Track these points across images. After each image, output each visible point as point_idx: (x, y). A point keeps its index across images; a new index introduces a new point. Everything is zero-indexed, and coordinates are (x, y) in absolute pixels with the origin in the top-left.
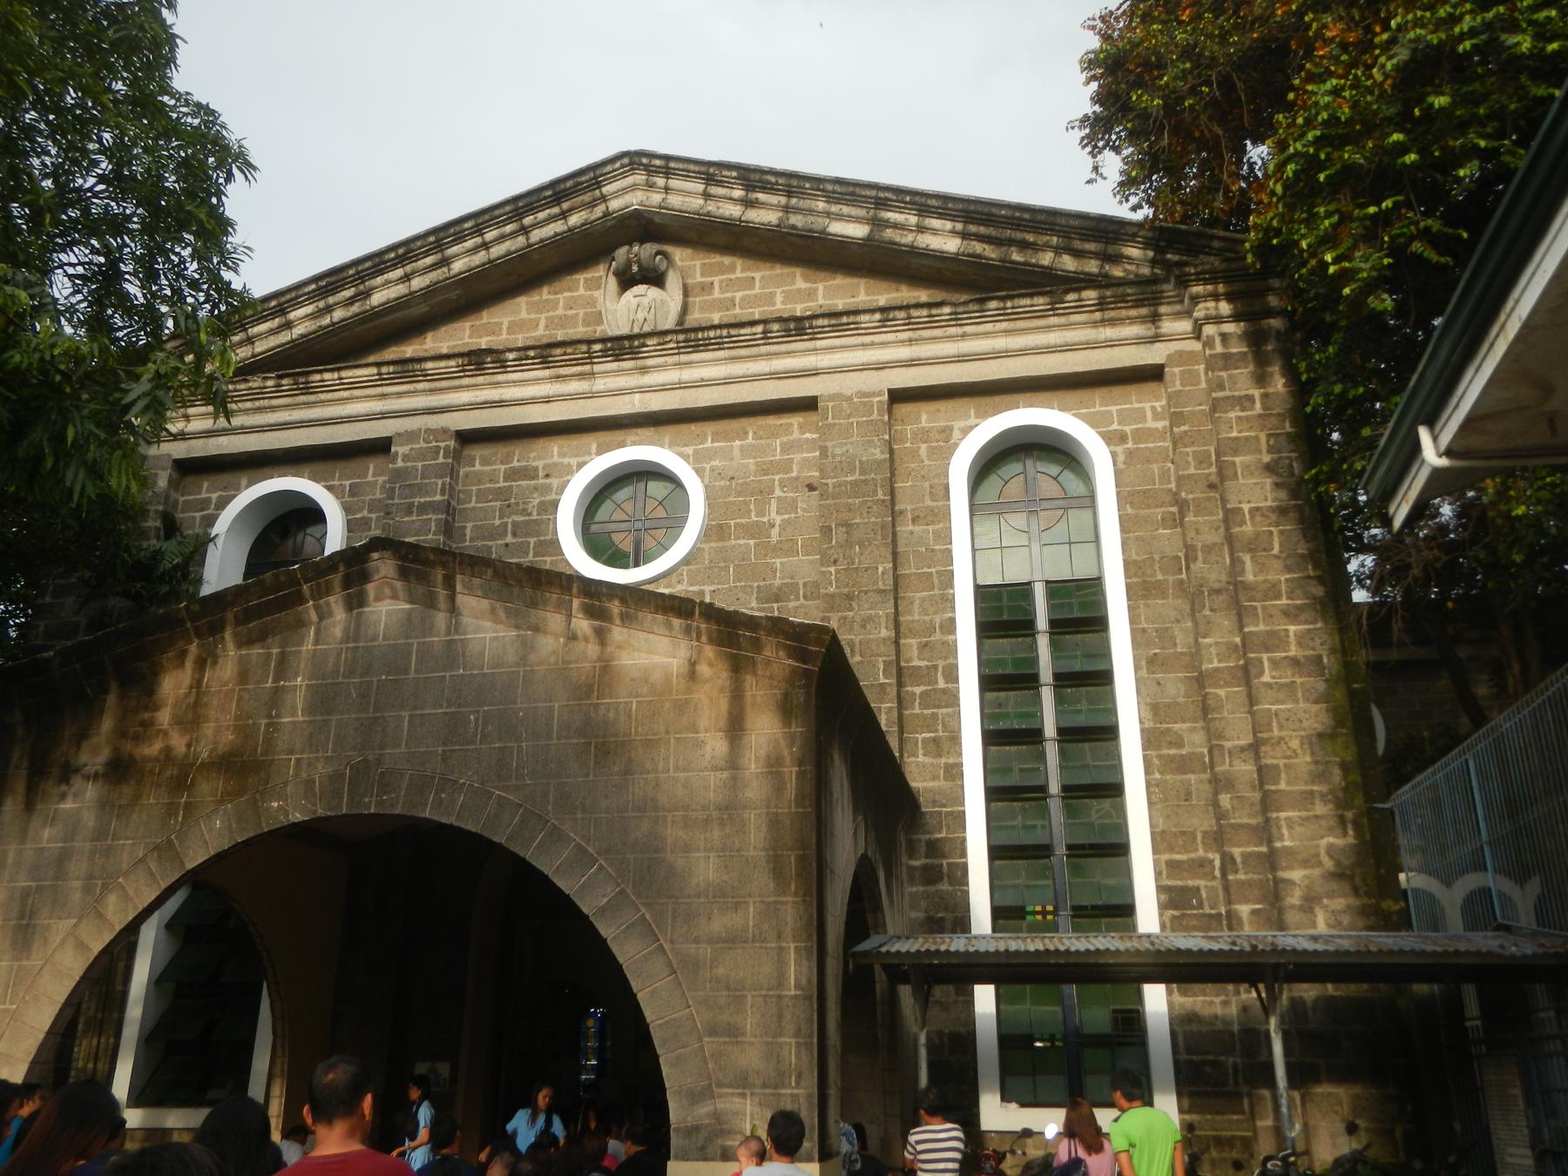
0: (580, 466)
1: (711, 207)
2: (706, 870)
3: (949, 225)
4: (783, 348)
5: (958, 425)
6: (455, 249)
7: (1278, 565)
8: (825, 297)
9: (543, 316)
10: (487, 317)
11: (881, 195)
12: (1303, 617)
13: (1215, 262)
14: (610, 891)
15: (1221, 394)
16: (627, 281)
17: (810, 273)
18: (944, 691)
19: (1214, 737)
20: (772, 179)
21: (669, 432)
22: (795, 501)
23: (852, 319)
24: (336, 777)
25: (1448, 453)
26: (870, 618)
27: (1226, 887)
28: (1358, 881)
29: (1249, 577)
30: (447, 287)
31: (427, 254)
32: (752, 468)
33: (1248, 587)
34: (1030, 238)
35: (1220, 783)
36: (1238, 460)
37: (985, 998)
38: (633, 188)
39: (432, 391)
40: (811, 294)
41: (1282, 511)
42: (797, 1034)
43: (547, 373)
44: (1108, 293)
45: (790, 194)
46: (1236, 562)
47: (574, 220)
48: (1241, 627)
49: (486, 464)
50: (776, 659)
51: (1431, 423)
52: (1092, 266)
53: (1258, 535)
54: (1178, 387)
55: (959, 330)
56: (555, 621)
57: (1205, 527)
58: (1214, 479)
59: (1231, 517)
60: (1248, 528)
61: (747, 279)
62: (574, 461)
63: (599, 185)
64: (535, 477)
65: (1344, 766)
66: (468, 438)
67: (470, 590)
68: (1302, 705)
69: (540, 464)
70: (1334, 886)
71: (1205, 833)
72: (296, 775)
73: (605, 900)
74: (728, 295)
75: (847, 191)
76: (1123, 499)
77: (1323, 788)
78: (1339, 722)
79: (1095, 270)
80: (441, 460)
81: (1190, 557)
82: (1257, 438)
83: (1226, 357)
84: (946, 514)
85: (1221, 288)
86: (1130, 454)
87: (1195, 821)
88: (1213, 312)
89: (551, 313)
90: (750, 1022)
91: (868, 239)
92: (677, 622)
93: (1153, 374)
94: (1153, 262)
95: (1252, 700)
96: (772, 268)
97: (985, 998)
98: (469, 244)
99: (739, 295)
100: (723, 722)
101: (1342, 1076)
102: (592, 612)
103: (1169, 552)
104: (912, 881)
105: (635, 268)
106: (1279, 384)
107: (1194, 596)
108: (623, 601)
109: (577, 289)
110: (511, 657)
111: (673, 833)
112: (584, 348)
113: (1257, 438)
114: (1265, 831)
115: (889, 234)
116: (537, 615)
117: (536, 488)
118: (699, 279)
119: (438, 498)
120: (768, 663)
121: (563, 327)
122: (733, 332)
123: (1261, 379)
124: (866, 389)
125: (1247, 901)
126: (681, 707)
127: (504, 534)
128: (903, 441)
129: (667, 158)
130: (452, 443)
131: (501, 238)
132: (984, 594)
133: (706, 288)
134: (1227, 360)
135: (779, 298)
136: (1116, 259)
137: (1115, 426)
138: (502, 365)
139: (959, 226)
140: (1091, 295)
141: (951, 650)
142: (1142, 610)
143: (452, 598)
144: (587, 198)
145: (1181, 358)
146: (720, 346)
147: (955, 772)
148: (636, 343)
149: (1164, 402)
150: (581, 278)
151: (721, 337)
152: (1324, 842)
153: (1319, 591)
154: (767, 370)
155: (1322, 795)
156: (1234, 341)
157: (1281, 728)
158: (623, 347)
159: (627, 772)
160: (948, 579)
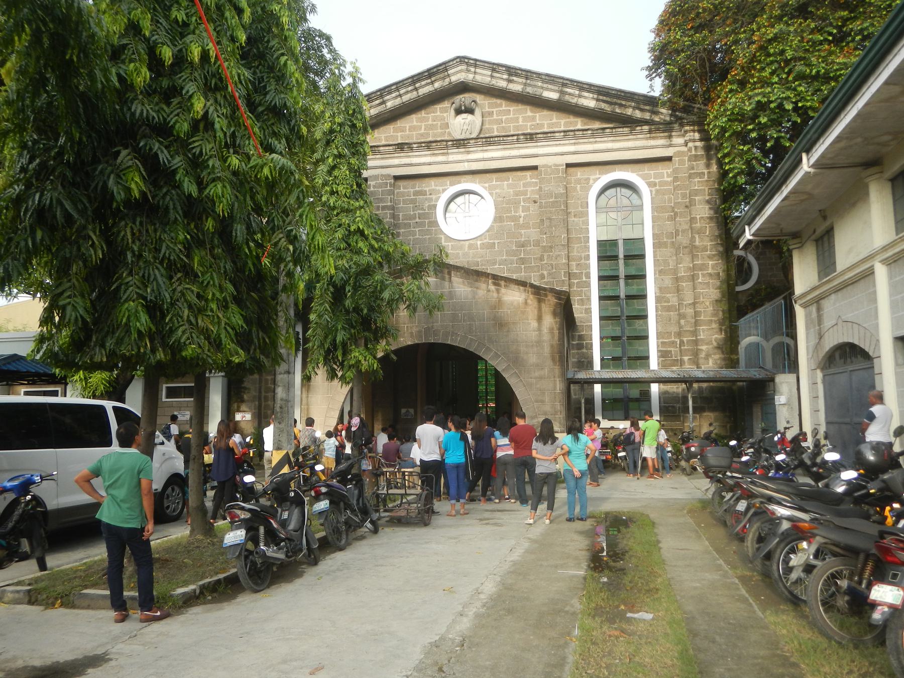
0: (444, 190)
1: (494, 82)
2: (532, 359)
3: (591, 95)
4: (525, 145)
5: (592, 177)
6: (388, 97)
7: (708, 239)
8: (539, 120)
10: (400, 123)
11: (565, 82)
12: (715, 258)
13: (695, 118)
14: (505, 365)
15: (693, 171)
16: (459, 112)
17: (534, 109)
18: (585, 282)
19: (681, 300)
20: (520, 72)
21: (478, 177)
22: (529, 207)
23: (552, 135)
24: (420, 332)
25: (753, 235)
26: (559, 255)
27: (681, 351)
28: (724, 349)
29: (697, 243)
31: (376, 99)
32: (512, 193)
33: (696, 247)
34: (624, 103)
35: (682, 316)
36: (696, 198)
37: (598, 388)
38: (461, 71)
39: (382, 158)
40: (534, 119)
41: (711, 218)
42: (560, 402)
43: (429, 152)
44: (653, 127)
45: (527, 79)
46: (693, 237)
47: (437, 85)
48: (693, 262)
49: (405, 188)
50: (552, 300)
51: (749, 224)
52: (647, 116)
53: (701, 227)
54: (677, 166)
55: (594, 140)
56: (484, 286)
57: (683, 223)
58: (688, 204)
59: (692, 220)
60: (698, 225)
62: (441, 188)
63: (447, 70)
64: (425, 195)
65: (723, 311)
66: (397, 178)
67: (456, 276)
68: (712, 290)
69: (427, 189)
70: (716, 351)
71: (675, 332)
72: (407, 330)
74: (500, 117)
75: (550, 79)
76: (654, 209)
77: (716, 319)
78: (723, 296)
79: (648, 118)
80: (389, 188)
81: (677, 234)
82: (704, 190)
83: (696, 156)
84: (587, 214)
85: (696, 128)
86: (657, 191)
87: (672, 328)
88: (692, 138)
90: (547, 399)
91: (559, 100)
92: (522, 288)
93: (669, 159)
94: (671, 115)
95: (694, 288)
96: (517, 106)
97: (598, 388)
98: (394, 95)
99: (504, 118)
100: (536, 317)
101: (712, 410)
102: (495, 284)
103: (670, 230)
104: (573, 349)
105: (463, 108)
106: (714, 168)
107: (677, 249)
108: (505, 281)
109: (437, 112)
110: (470, 296)
111: (523, 349)
112: (445, 143)
113: (704, 190)
114: (695, 333)
115: (567, 98)
116: (477, 284)
117: (426, 199)
118: (487, 110)
119: (389, 204)
120: (549, 300)
121: (432, 129)
122: (505, 139)
123: (708, 166)
124: (557, 163)
125: (687, 356)
126: (523, 313)
127: (415, 218)
128: (571, 183)
129: (476, 60)
130: (392, 181)
131: (407, 92)
132: (601, 244)
133: (490, 114)
134: (696, 158)
135: (521, 120)
136: (656, 113)
137: (652, 180)
138: (411, 149)
139: (595, 96)
140: (646, 128)
141: (588, 266)
142: (658, 253)
143: (450, 278)
144: (442, 75)
145: (679, 154)
146: (499, 144)
147: (589, 311)
149: (671, 170)
150: (438, 107)
152: (714, 337)
153: (721, 249)
154: (518, 154)
155: (715, 321)
156: (699, 149)
157: (703, 298)
158: (460, 143)
159: (508, 331)
160: (587, 239)
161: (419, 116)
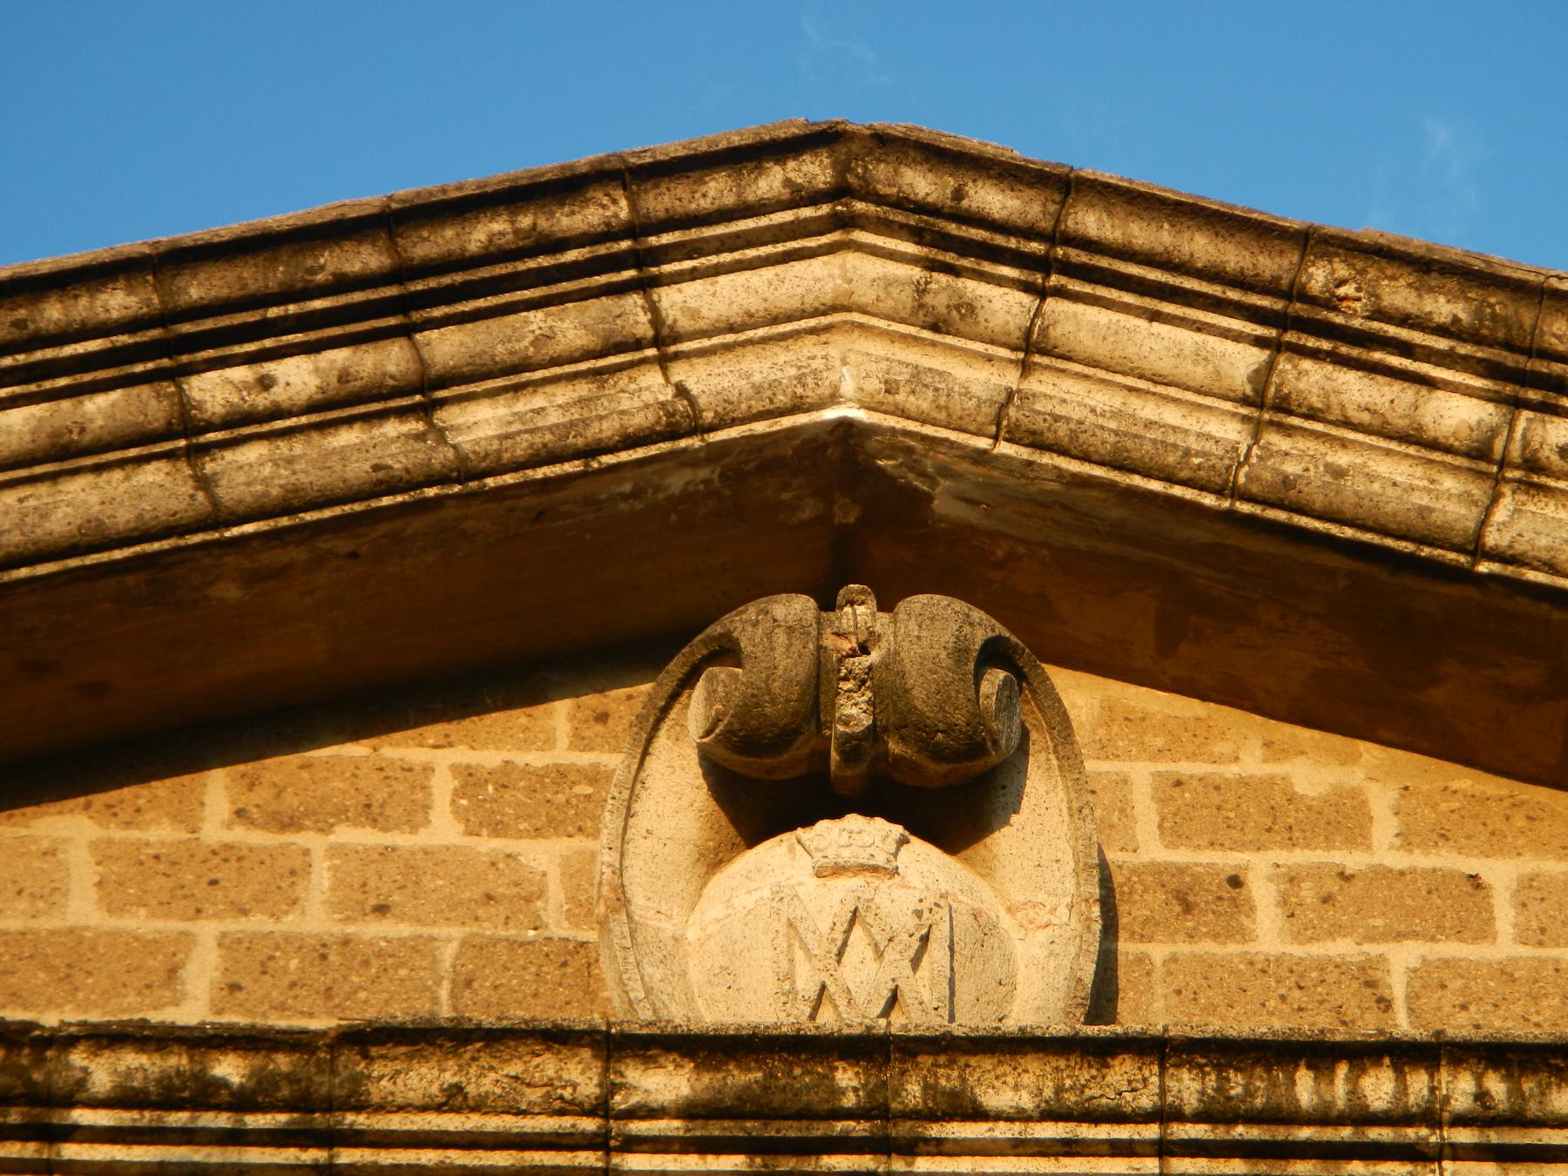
9: (207, 931)
61: (1438, 882)
89: (257, 923)
148: (913, 1092)
151: (1429, 1117)
161: (161, 833)
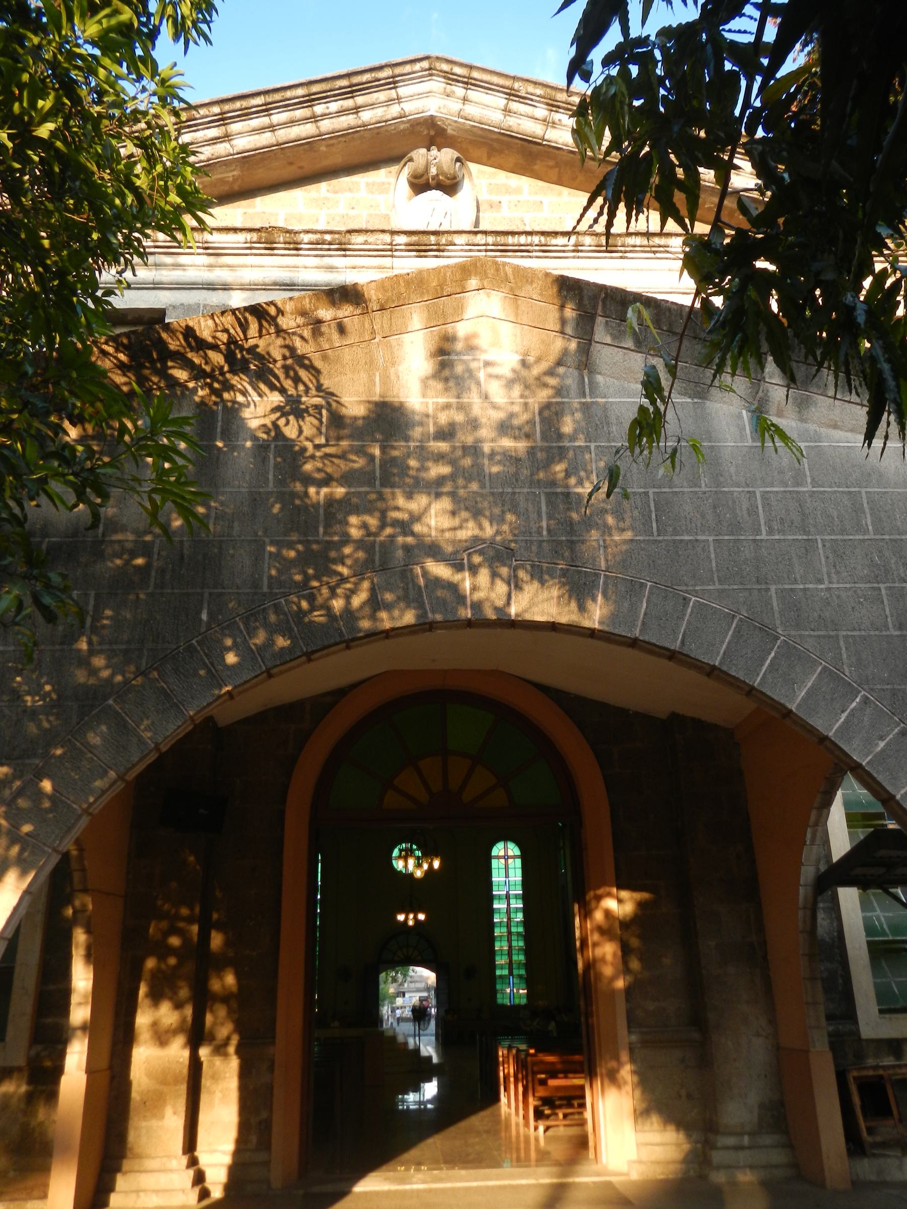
30: (226, 164)
73: (882, 744)
98: (255, 123)
148: (444, 241)
